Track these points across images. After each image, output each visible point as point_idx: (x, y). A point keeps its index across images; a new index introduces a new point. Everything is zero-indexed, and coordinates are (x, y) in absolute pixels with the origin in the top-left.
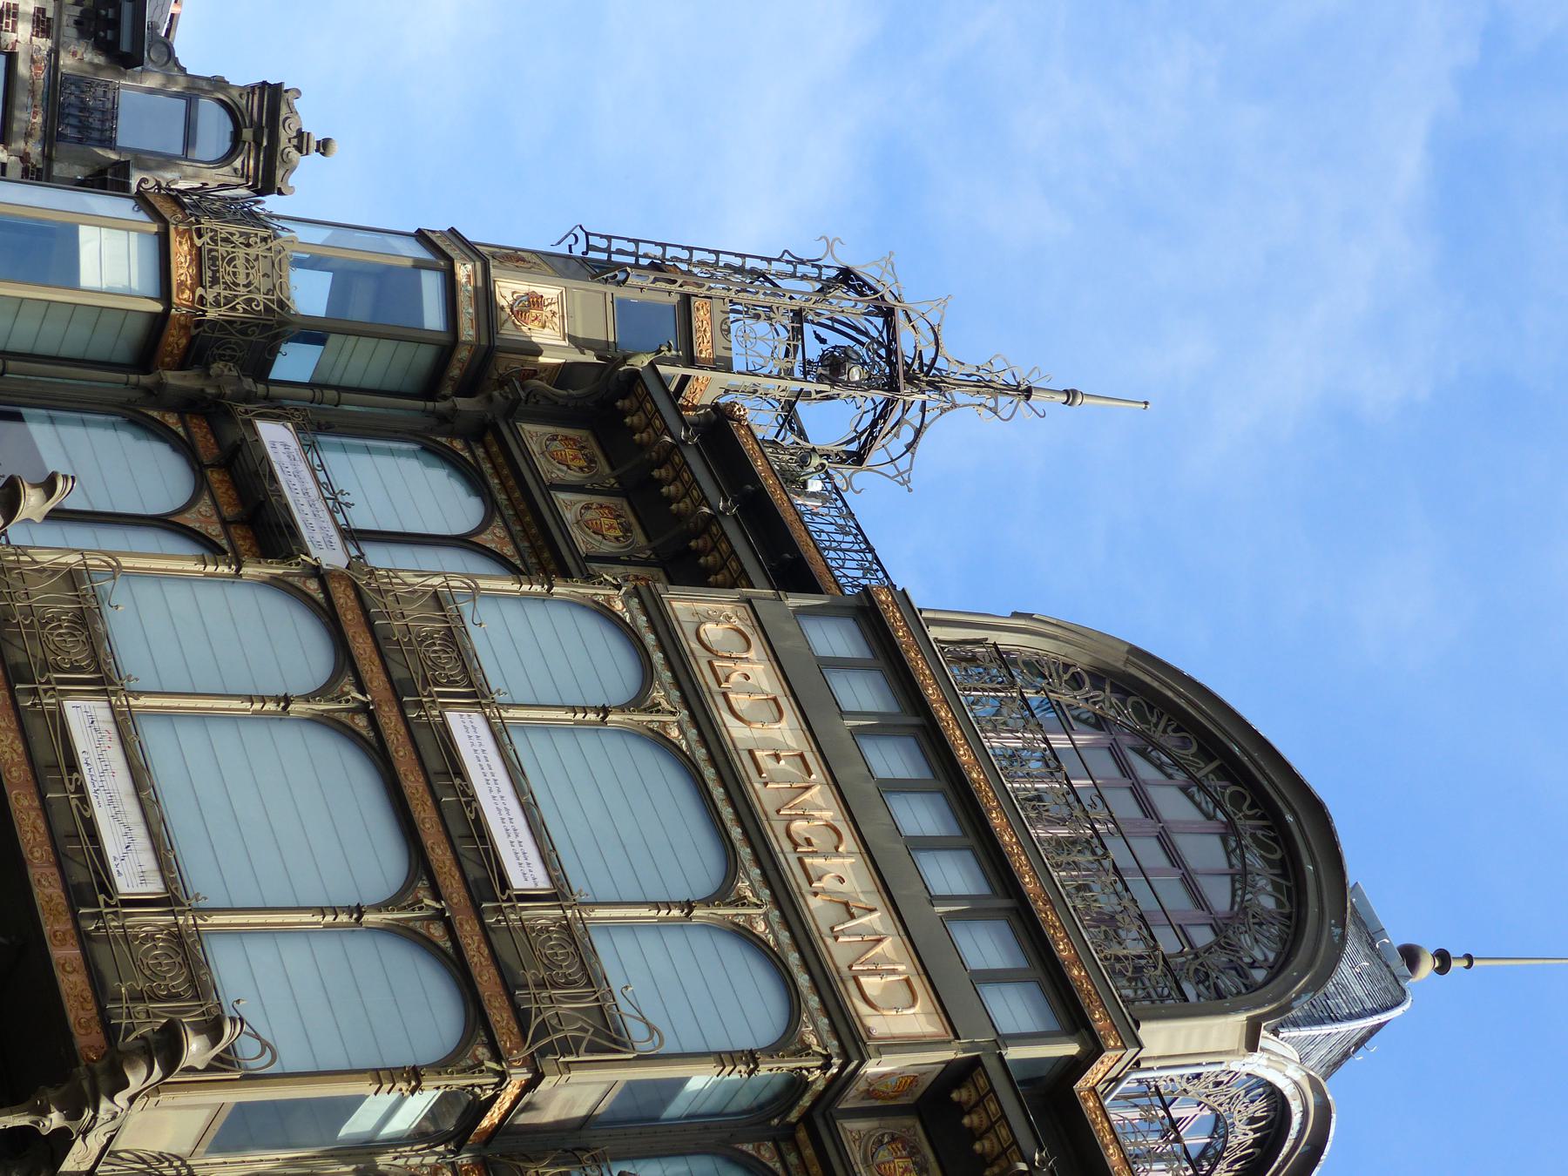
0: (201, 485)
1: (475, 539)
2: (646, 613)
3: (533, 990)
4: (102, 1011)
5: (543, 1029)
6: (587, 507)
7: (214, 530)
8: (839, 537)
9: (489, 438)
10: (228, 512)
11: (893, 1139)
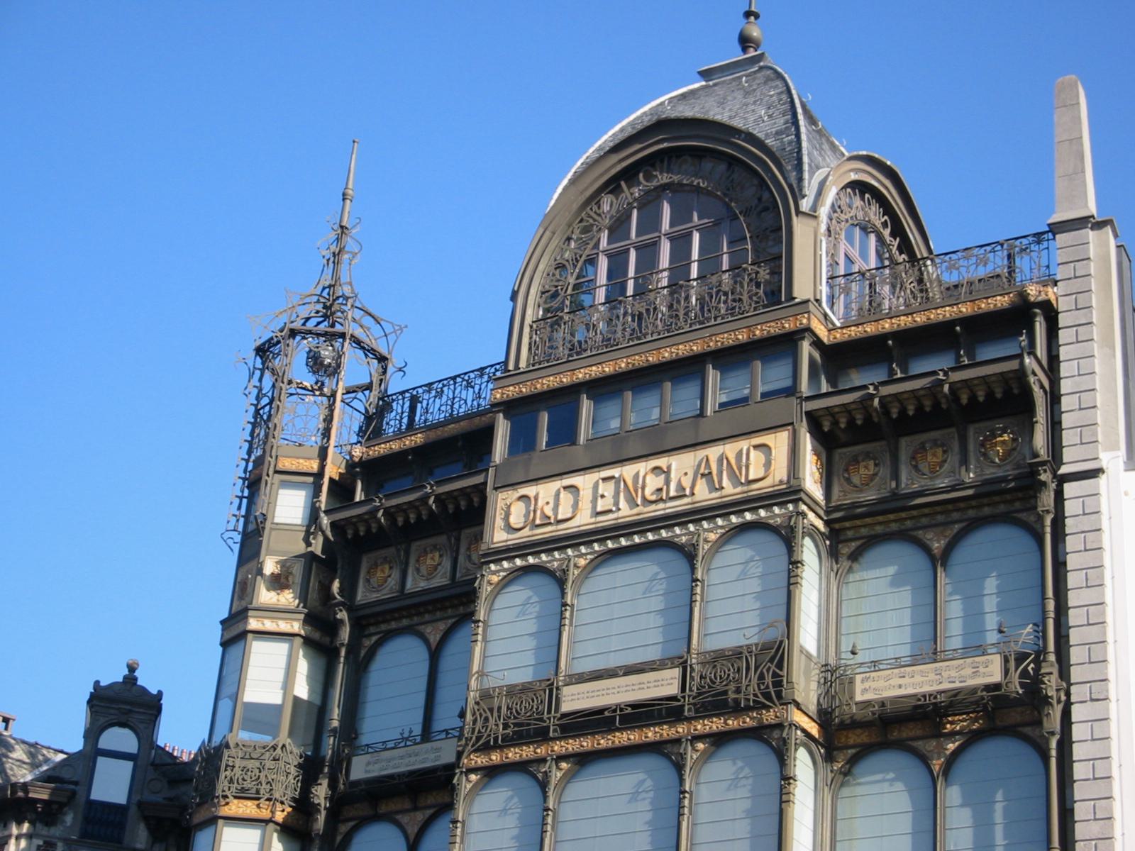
0: (389, 818)
3: (742, 696)
5: (767, 696)
6: (418, 570)
7: (420, 816)
8: (444, 398)
9: (364, 622)
11: (847, 470)
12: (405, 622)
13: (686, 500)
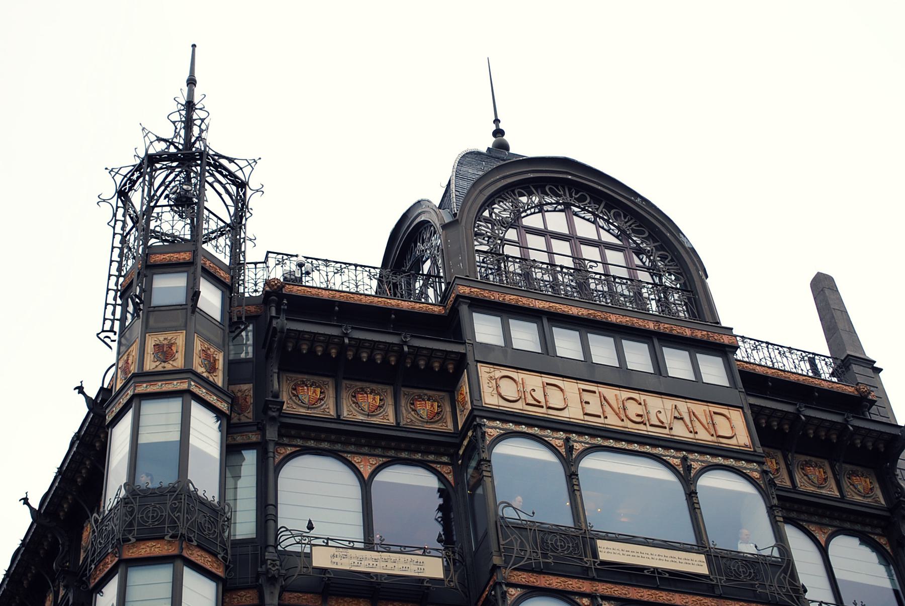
1: (366, 476)
2: (495, 419)
8: (345, 278)
12: (325, 445)
13: (667, 431)
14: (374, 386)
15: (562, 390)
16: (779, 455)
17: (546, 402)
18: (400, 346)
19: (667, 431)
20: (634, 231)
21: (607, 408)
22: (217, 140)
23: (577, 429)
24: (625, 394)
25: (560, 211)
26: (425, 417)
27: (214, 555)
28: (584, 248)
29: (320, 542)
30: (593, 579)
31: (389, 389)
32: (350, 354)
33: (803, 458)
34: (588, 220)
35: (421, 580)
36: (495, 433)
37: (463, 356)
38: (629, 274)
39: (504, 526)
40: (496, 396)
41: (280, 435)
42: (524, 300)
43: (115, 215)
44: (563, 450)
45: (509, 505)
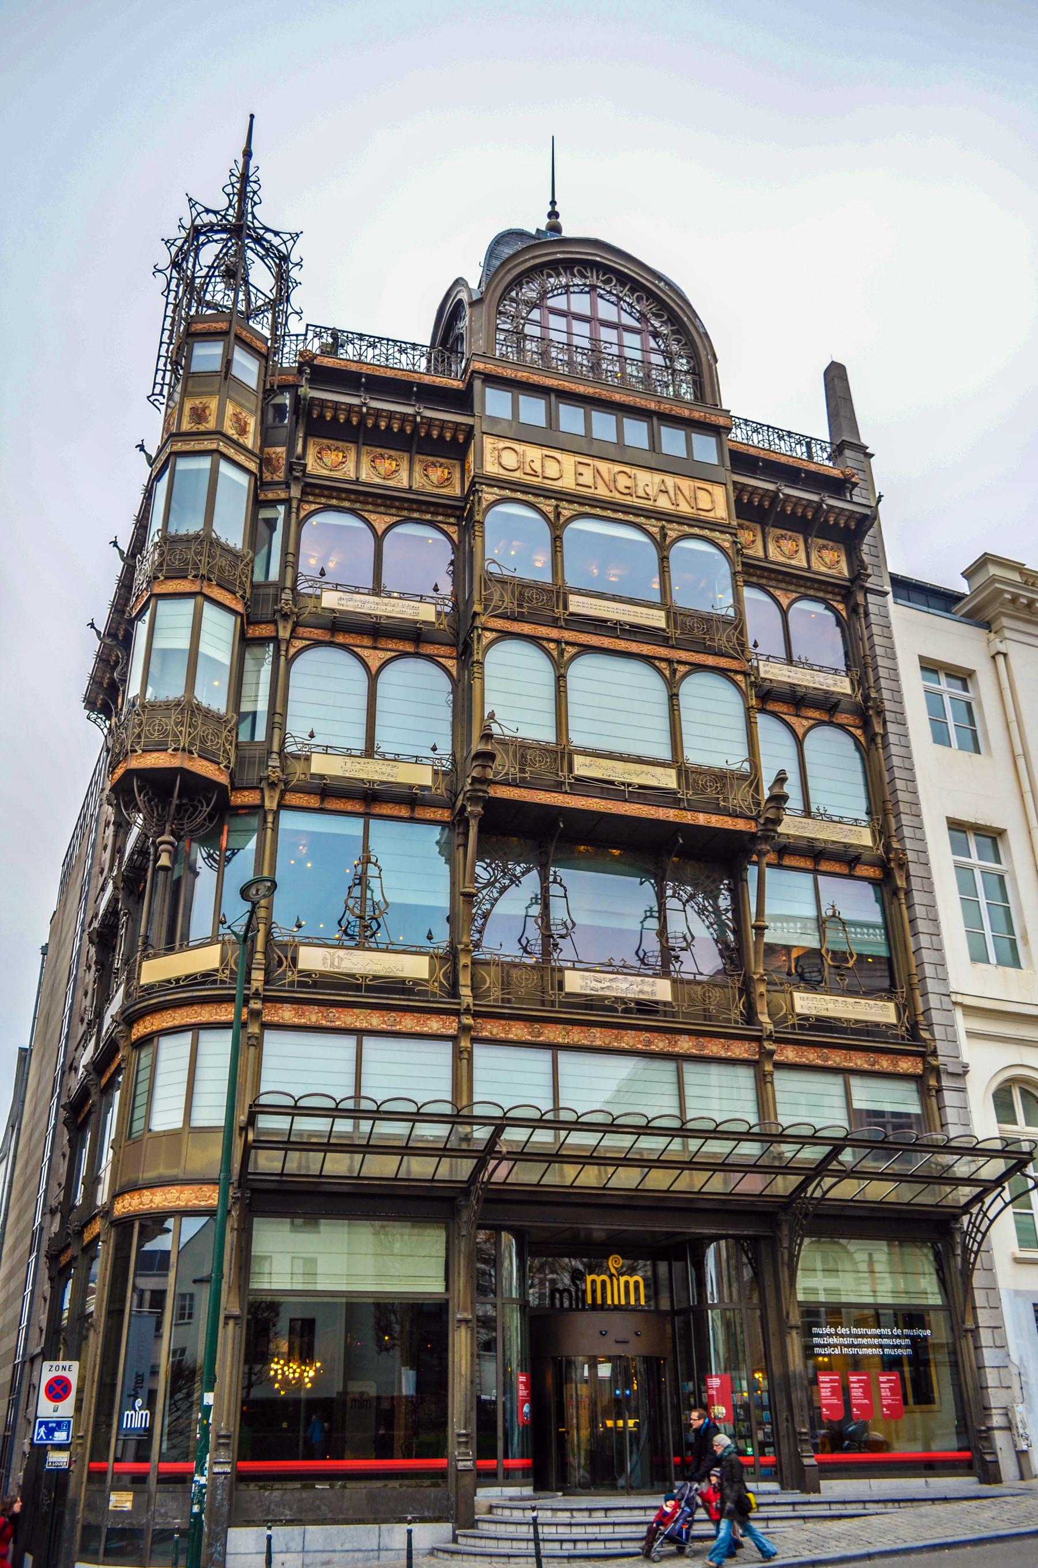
1: (380, 533)
4: (730, 815)
8: (377, 351)
10: (367, 641)
12: (347, 504)
13: (651, 503)
14: (392, 453)
15: (559, 462)
16: (758, 527)
17: (543, 472)
18: (415, 416)
19: (651, 503)
20: (654, 314)
21: (599, 481)
22: (267, 213)
23: (568, 498)
24: (618, 468)
25: (586, 293)
26: (435, 481)
27: (234, 593)
28: (603, 329)
29: (330, 586)
30: (561, 627)
31: (406, 456)
32: (370, 423)
33: (780, 532)
34: (612, 303)
35: (416, 622)
36: (492, 498)
37: (472, 427)
38: (643, 356)
39: (490, 579)
40: (497, 465)
41: (304, 493)
42: (535, 378)
43: (168, 285)
44: (552, 516)
45: (494, 562)
